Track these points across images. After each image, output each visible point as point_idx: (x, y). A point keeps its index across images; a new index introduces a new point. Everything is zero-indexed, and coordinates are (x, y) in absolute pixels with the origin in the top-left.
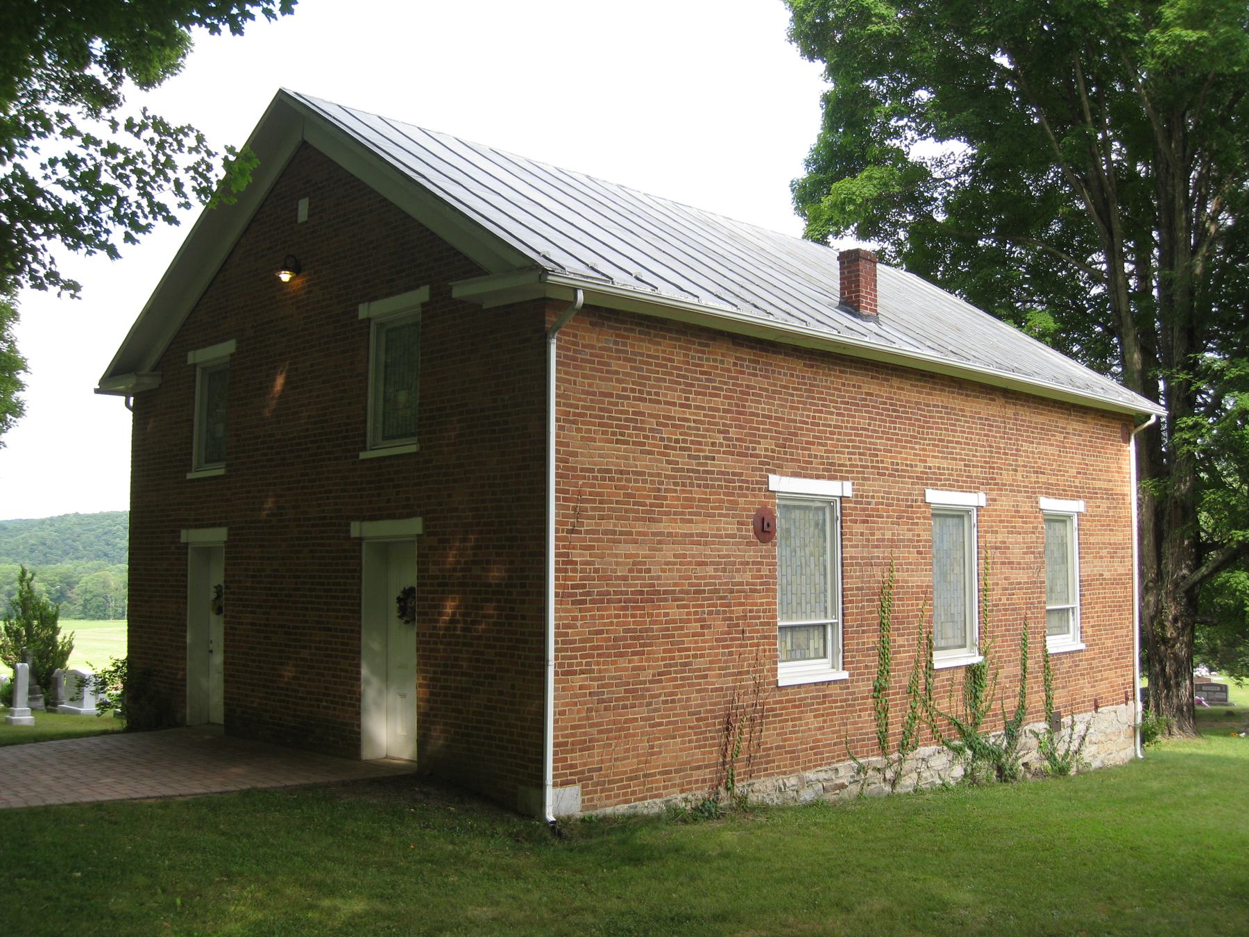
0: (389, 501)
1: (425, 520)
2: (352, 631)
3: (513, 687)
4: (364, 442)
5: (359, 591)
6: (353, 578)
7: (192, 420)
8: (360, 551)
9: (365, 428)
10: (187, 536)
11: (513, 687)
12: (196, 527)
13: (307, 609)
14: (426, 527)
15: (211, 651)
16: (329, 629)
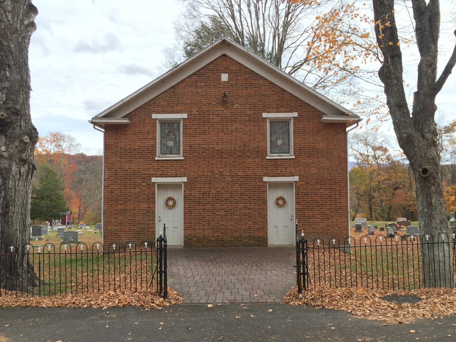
0: (282, 171)
1: (299, 177)
2: (263, 209)
3: (337, 220)
4: (267, 154)
5: (266, 197)
6: (264, 193)
7: (156, 139)
8: (266, 186)
9: (267, 150)
10: (154, 180)
11: (337, 220)
12: (162, 177)
13: (238, 203)
14: (299, 179)
15: (160, 220)
16: (252, 209)
